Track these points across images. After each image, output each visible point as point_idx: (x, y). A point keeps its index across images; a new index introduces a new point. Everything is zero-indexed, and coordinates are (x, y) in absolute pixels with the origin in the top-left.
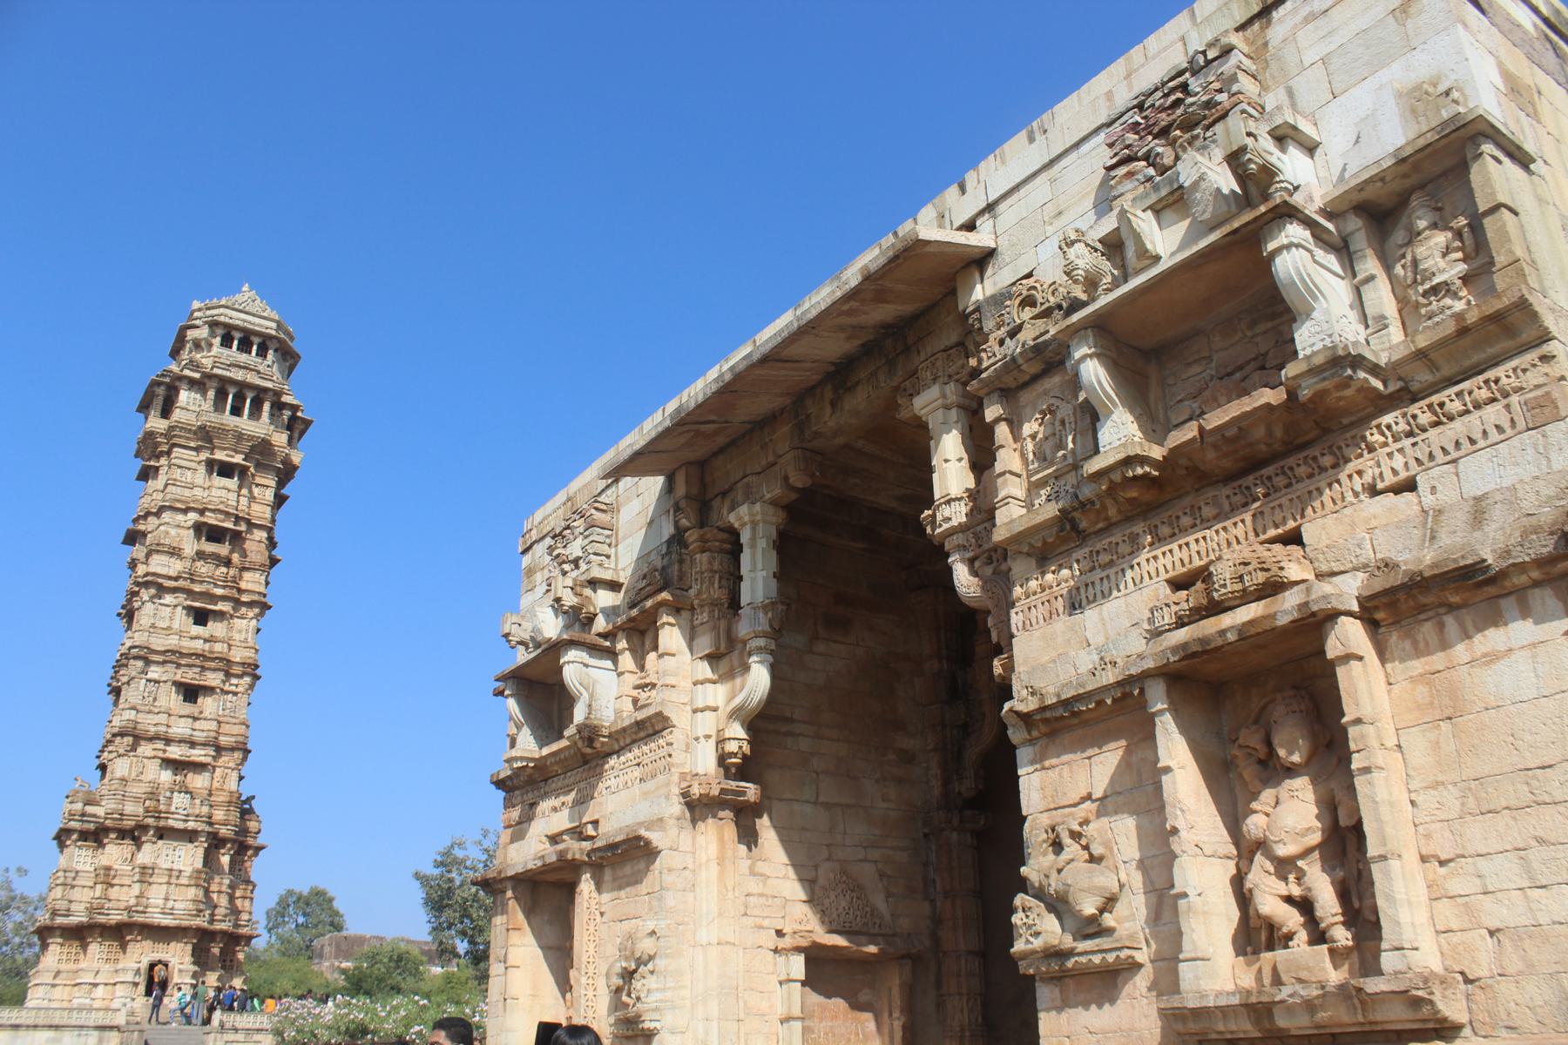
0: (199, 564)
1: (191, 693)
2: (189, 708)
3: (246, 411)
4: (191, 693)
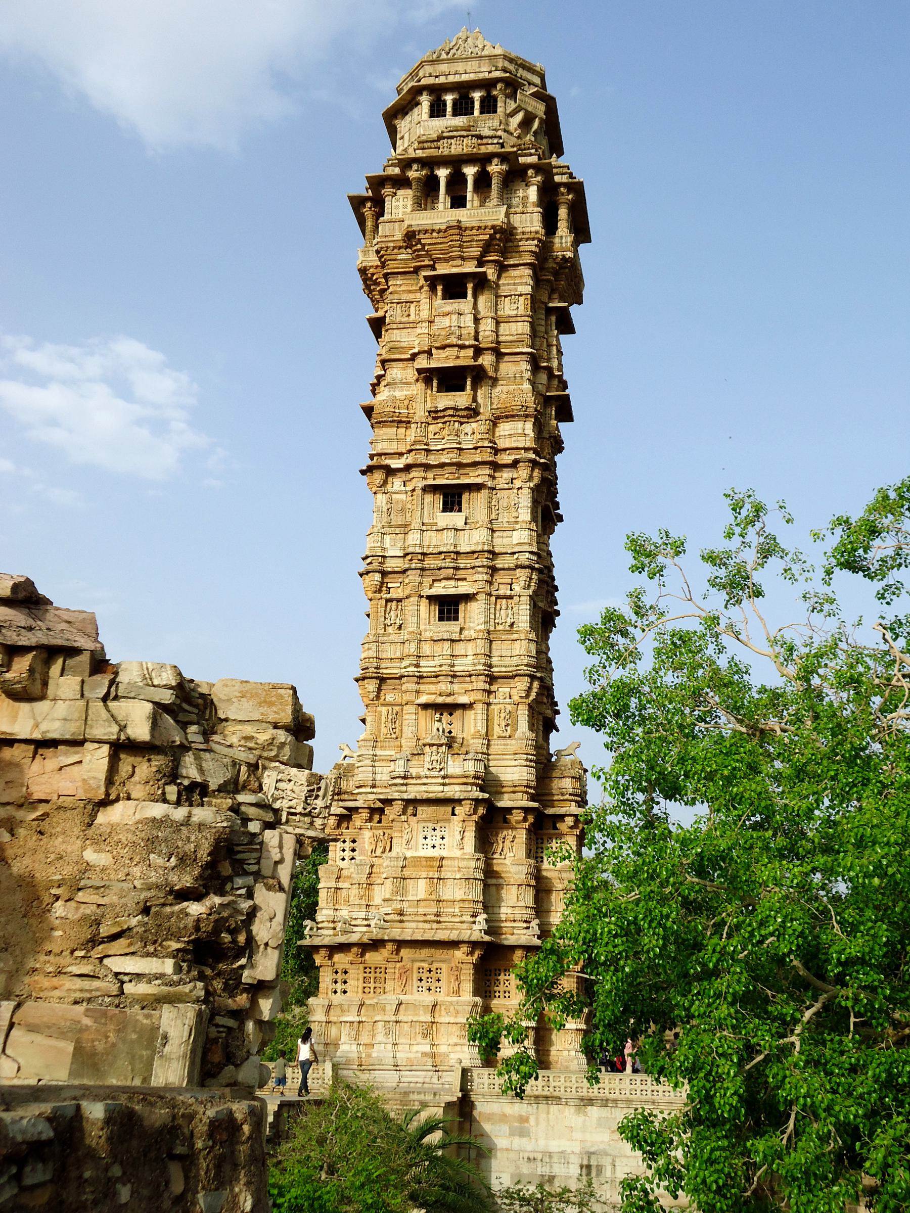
0: (431, 428)
1: (448, 607)
2: (450, 628)
3: (469, 196)
4: (448, 607)
